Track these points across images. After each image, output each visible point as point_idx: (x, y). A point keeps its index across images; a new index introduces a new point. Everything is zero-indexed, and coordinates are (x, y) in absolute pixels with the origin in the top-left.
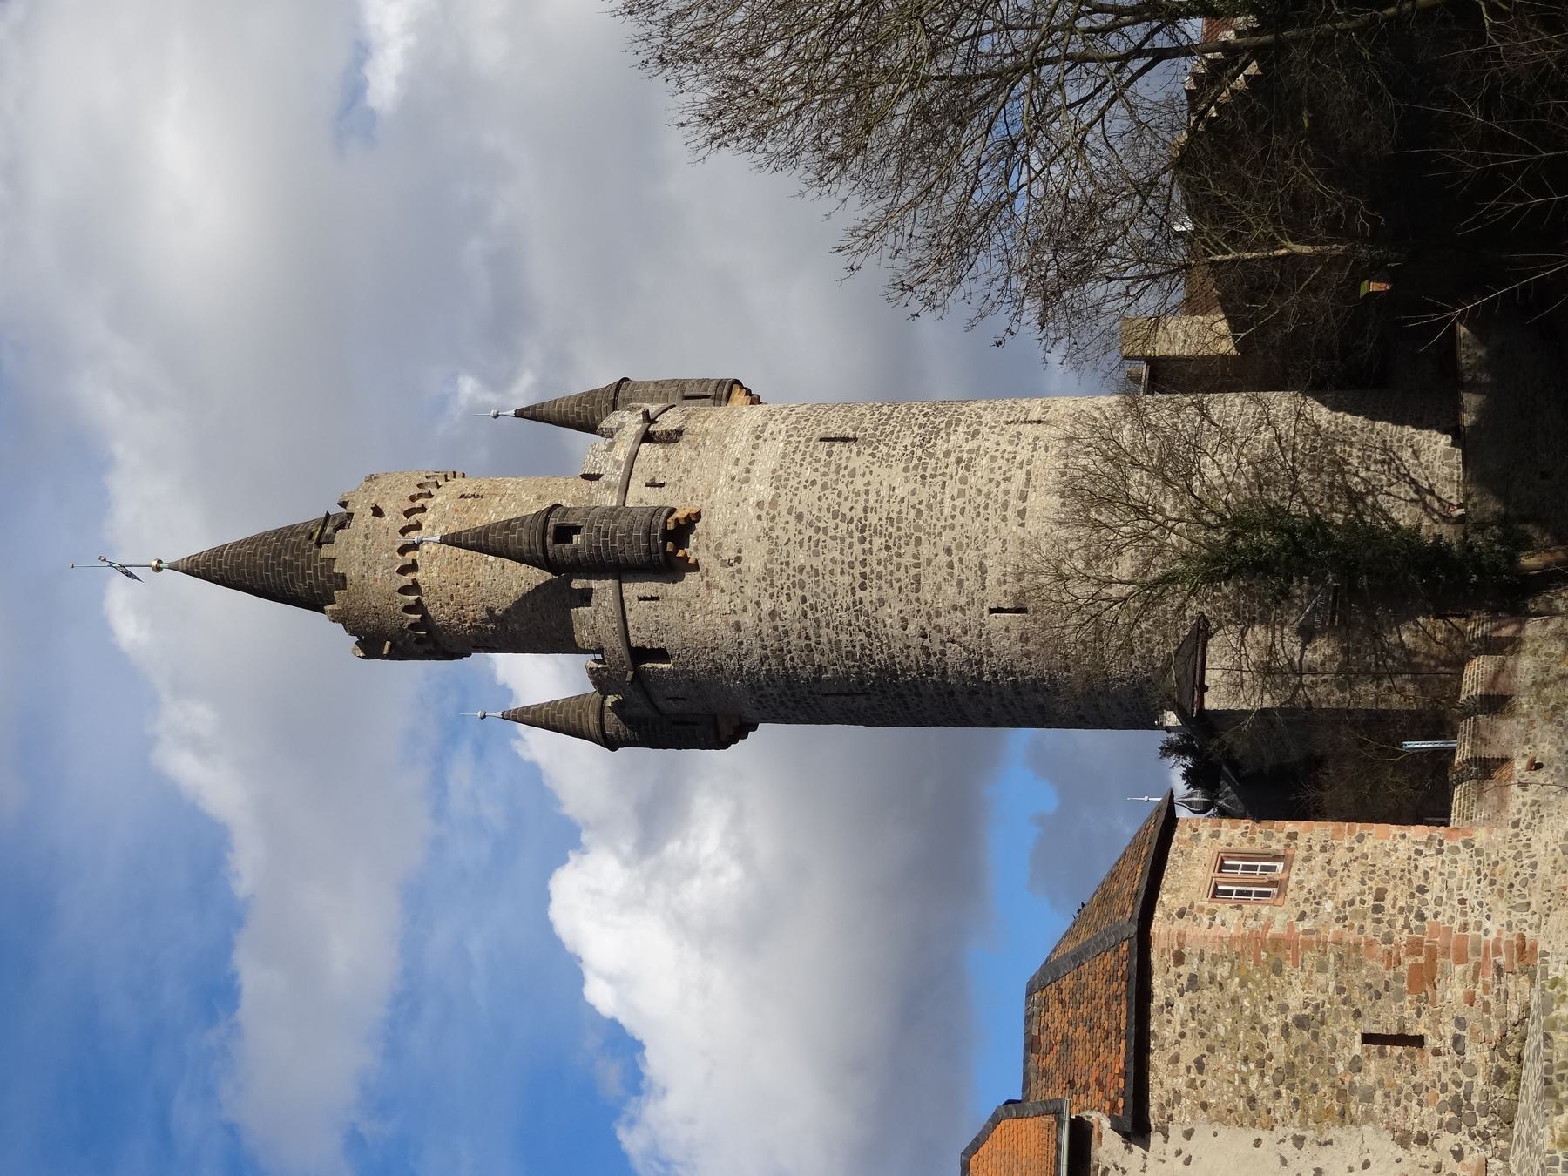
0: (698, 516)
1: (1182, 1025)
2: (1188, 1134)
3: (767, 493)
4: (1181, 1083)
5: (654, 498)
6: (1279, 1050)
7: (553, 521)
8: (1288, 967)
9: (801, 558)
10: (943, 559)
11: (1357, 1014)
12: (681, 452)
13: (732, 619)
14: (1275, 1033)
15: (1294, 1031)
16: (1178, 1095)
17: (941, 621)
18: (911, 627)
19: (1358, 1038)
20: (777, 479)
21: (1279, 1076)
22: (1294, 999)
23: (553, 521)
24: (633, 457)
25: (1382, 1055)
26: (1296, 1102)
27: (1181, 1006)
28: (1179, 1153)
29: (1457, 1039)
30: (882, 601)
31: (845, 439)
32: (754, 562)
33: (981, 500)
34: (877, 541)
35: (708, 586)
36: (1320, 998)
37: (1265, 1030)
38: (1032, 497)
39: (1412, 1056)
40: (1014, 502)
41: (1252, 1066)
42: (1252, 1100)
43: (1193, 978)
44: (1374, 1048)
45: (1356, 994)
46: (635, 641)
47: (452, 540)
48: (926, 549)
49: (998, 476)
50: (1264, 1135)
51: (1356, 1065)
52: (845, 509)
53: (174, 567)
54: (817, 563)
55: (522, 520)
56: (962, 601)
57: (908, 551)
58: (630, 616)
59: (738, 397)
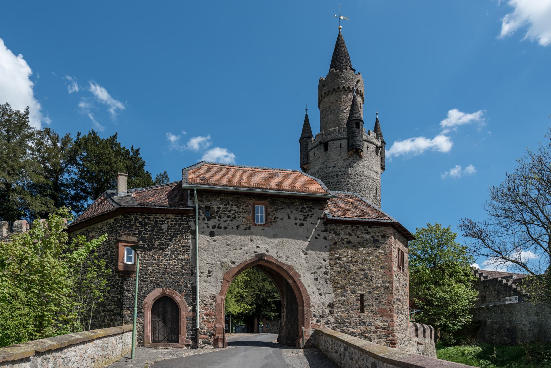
1: (362, 237)
2: (325, 238)
4: (342, 236)
5: (365, 147)
11: (370, 293)
13: (336, 166)
14: (361, 267)
16: (338, 235)
19: (362, 293)
21: (348, 267)
25: (357, 300)
28: (319, 235)
29: (364, 323)
35: (344, 160)
37: (362, 264)
39: (358, 309)
41: (350, 259)
42: (339, 258)
44: (359, 298)
46: (329, 143)
50: (327, 263)
58: (336, 142)
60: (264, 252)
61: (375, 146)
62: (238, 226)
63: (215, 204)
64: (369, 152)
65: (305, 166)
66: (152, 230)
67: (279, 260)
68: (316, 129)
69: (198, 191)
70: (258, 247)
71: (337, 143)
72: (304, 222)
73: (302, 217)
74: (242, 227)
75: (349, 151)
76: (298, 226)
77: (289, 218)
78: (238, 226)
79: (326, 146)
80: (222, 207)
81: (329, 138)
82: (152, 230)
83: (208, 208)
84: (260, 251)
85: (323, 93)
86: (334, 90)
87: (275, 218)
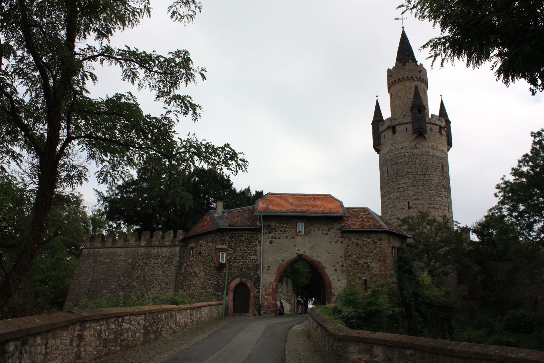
0: (426, 139)
2: (342, 242)
3: (431, 153)
5: (428, 129)
6: (362, 261)
7: (422, 108)
8: (380, 263)
9: (418, 161)
10: (419, 191)
11: (371, 278)
12: (438, 135)
14: (365, 261)
15: (366, 265)
17: (406, 192)
18: (403, 185)
20: (434, 156)
22: (373, 265)
23: (422, 108)
24: (436, 125)
25: (363, 284)
26: (351, 265)
27: (369, 240)
30: (409, 178)
31: (443, 169)
32: (415, 151)
33: (432, 199)
34: (422, 177)
36: (374, 270)
37: (366, 259)
38: (434, 210)
40: (432, 206)
42: (350, 256)
43: (376, 243)
45: (376, 278)
46: (397, 127)
47: (416, 87)
48: (421, 187)
49: (438, 202)
50: (343, 259)
51: (360, 278)
52: (429, 170)
53: (403, 31)
54: (417, 165)
55: (422, 102)
56: (410, 195)
57: (421, 184)
59: (449, 147)
60: (302, 253)
61: (438, 127)
62: (287, 237)
63: (273, 224)
64: (433, 133)
65: (378, 147)
66: (236, 241)
67: (312, 258)
68: (386, 114)
69: (263, 216)
70: (299, 250)
71: (403, 127)
72: (329, 232)
73: (327, 229)
74: (290, 237)
75: (414, 134)
76: (324, 235)
77: (319, 230)
78: (287, 237)
79: (393, 129)
80: (277, 225)
81: (396, 122)
82: (236, 241)
83: (269, 226)
84: (301, 252)
85: (390, 82)
86: (399, 79)
87: (310, 230)
